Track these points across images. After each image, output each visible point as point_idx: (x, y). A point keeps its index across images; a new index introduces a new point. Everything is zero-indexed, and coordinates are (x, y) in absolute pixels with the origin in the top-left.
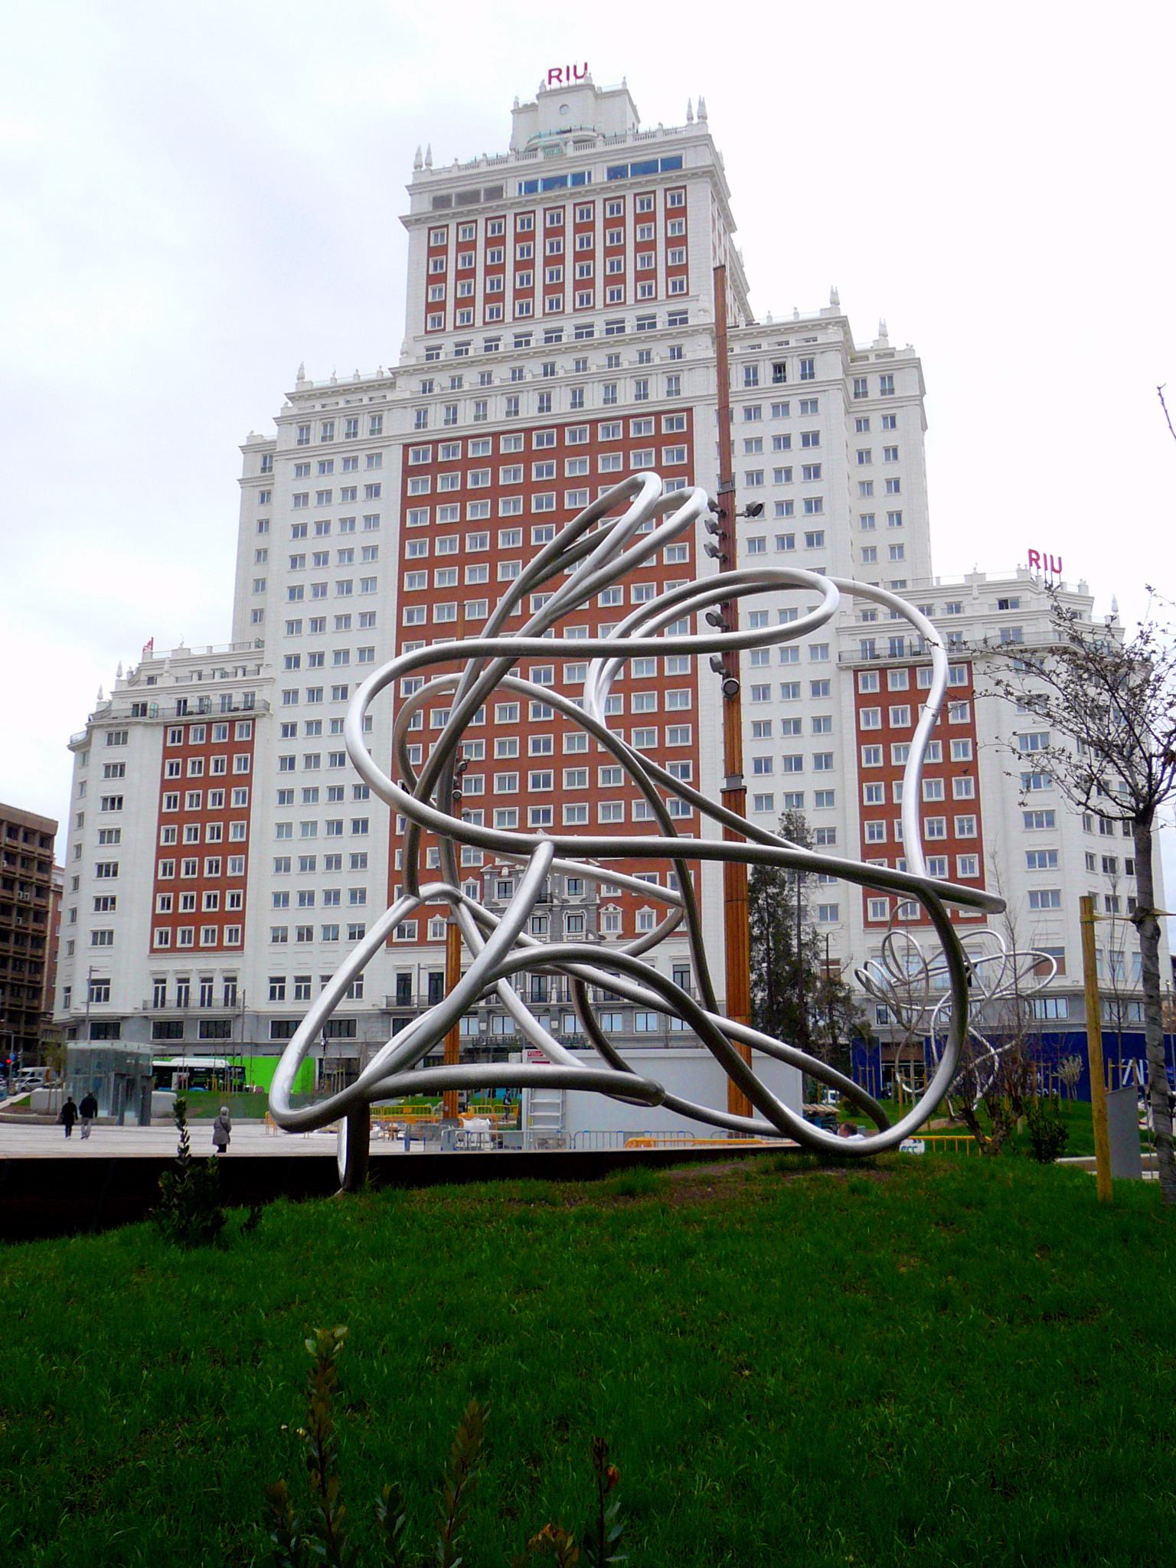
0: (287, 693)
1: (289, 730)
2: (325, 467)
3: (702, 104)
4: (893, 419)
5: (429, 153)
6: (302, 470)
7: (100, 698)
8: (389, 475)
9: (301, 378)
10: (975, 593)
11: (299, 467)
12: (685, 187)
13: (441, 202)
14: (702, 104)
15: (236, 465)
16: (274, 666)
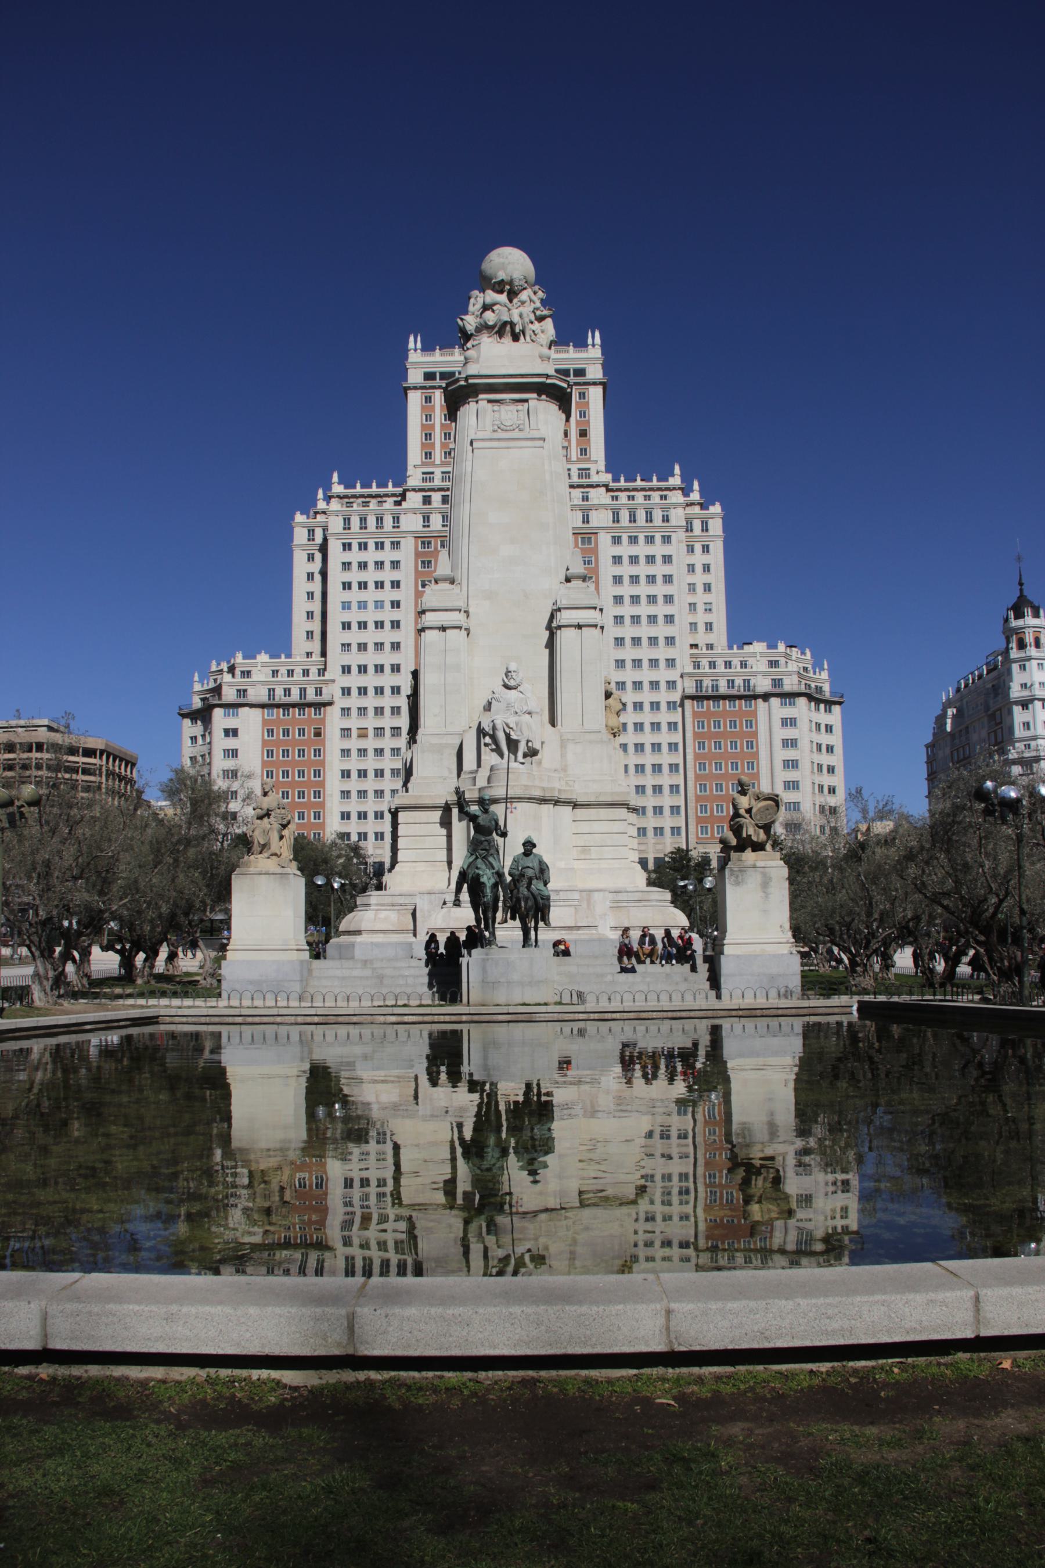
0: (343, 689)
1: (346, 711)
4: (708, 546)
6: (346, 547)
8: (407, 552)
10: (758, 658)
11: (344, 545)
13: (429, 376)
16: (333, 671)
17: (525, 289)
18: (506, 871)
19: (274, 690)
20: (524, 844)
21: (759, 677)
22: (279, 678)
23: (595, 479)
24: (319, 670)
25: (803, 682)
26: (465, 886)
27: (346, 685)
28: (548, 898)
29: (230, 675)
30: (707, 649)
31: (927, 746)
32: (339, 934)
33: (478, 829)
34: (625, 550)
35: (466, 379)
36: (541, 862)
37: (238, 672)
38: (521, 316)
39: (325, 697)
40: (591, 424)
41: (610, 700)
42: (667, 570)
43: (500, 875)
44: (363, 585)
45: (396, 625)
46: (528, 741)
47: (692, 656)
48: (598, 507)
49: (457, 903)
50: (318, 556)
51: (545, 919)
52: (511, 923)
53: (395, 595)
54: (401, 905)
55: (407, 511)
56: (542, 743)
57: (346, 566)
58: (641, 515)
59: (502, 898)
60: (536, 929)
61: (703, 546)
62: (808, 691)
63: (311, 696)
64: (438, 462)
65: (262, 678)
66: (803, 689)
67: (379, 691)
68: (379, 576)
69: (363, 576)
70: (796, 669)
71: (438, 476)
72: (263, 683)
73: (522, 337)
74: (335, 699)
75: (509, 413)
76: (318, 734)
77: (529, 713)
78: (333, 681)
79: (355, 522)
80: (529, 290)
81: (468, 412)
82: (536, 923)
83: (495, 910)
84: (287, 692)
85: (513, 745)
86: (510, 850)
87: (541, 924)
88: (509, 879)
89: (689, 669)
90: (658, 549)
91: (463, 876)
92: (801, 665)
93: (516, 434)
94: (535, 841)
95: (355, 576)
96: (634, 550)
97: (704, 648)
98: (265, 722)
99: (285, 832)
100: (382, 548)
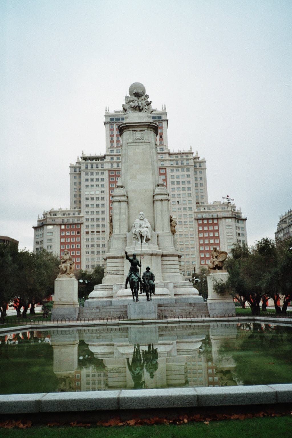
1: (87, 226)
2: (92, 174)
3: (165, 106)
4: (201, 171)
5: (108, 108)
6: (87, 174)
7: (38, 217)
8: (106, 176)
9: (83, 153)
10: (218, 206)
11: (86, 173)
12: (162, 123)
13: (112, 119)
14: (165, 106)
15: (68, 170)
17: (143, 95)
18: (141, 277)
19: (64, 220)
20: (147, 269)
21: (219, 213)
22: (66, 216)
23: (165, 151)
24: (79, 213)
25: (233, 214)
26: (129, 283)
27: (87, 217)
28: (154, 285)
29: (49, 215)
30: (202, 204)
31: (275, 233)
32: (88, 298)
33: (132, 264)
34: (175, 173)
35: (126, 123)
36: (152, 274)
37: (52, 214)
38: (142, 104)
39: (80, 222)
40: (164, 133)
41: (172, 223)
42: (188, 179)
43: (139, 278)
44: (92, 186)
45: (103, 198)
46: (147, 236)
47: (197, 206)
48: (166, 160)
49: (126, 288)
50: (78, 177)
51: (154, 292)
52: (143, 294)
53: (103, 189)
54: (108, 289)
55: (106, 163)
56: (151, 236)
57: (87, 180)
58: (180, 163)
59: (140, 286)
60: (151, 295)
61: (200, 171)
62: (235, 216)
63: (76, 221)
64: (115, 147)
65: (60, 216)
66: (233, 216)
67: (98, 219)
68: (97, 183)
69: (92, 183)
70: (231, 210)
71: (115, 151)
72: (60, 218)
73: (142, 111)
74: (84, 222)
75: (138, 135)
76: (78, 233)
77: (147, 227)
78: (83, 217)
79: (89, 166)
80: (144, 96)
81: (127, 134)
82: (151, 294)
83: (138, 290)
84: (68, 220)
85: (142, 236)
86: (142, 270)
87: (152, 294)
88: (142, 279)
89: (197, 211)
90: (186, 173)
91: (128, 279)
92: (232, 208)
93: (141, 141)
94: (150, 267)
95: (89, 183)
96: (178, 173)
97: (201, 204)
98: (62, 230)
99: (72, 267)
100: (98, 174)
